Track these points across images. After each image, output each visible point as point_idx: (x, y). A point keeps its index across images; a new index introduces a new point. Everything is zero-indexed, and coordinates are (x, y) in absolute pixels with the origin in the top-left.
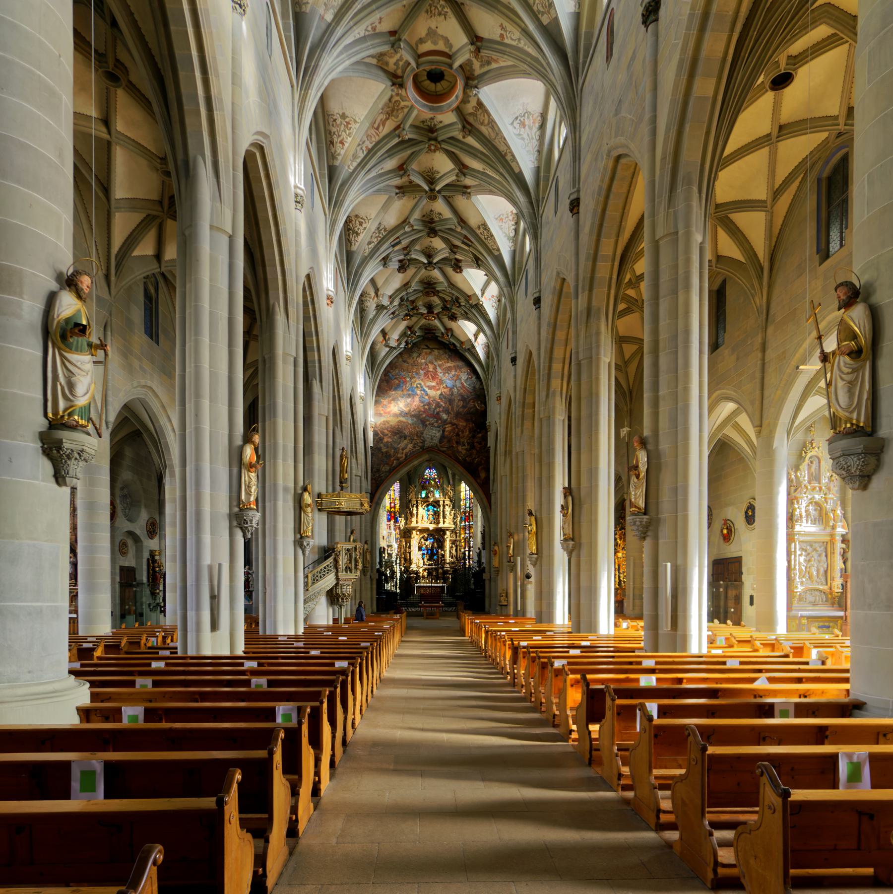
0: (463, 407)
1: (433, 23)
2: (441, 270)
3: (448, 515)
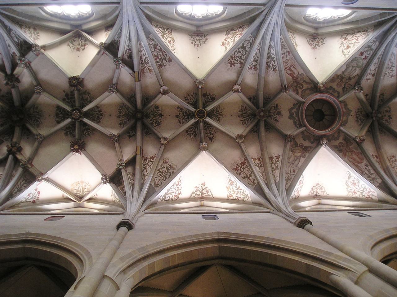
1: (353, 113)
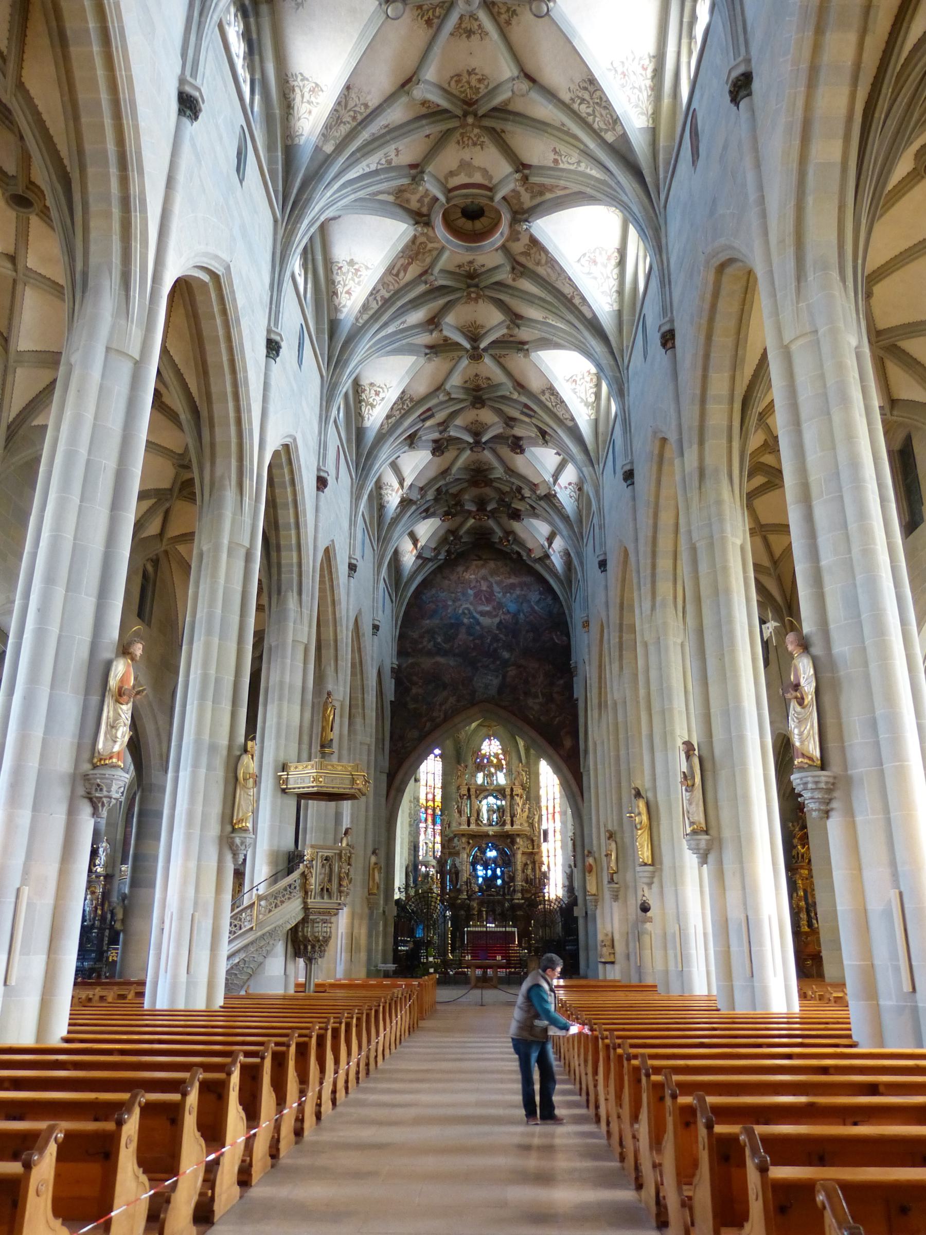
1: (466, 154)
2: (494, 451)
3: (519, 810)
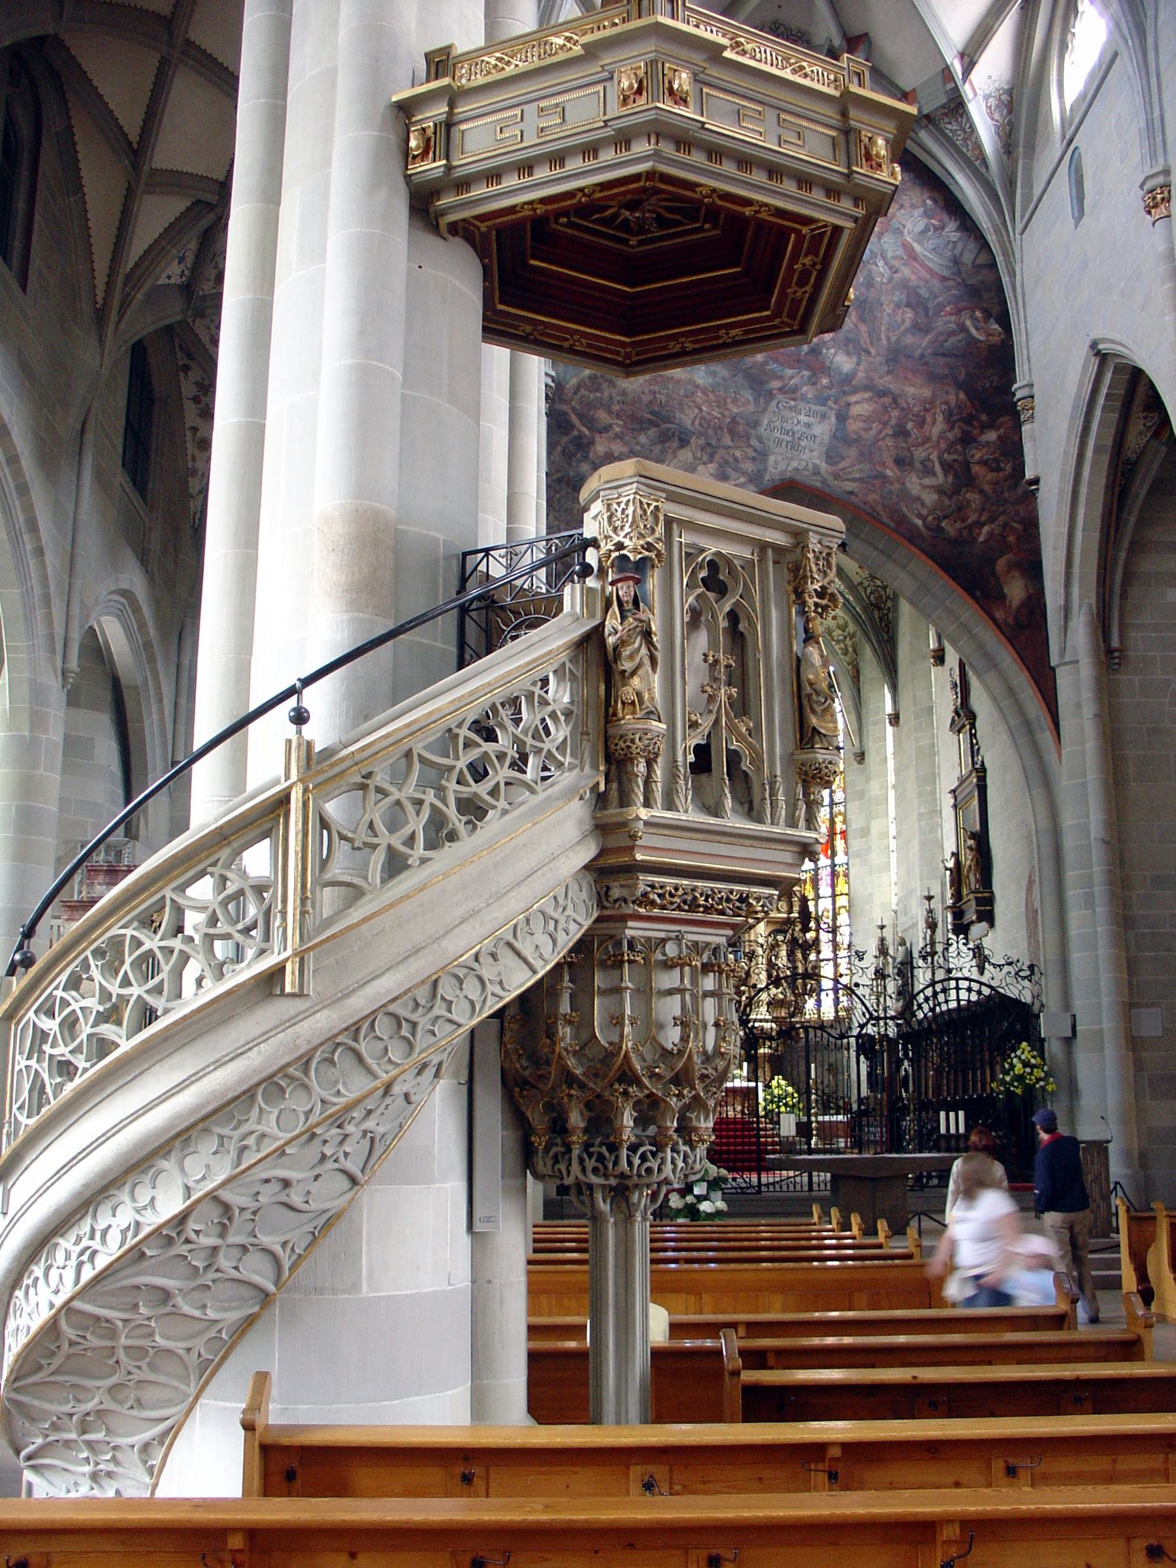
0: (916, 327)
